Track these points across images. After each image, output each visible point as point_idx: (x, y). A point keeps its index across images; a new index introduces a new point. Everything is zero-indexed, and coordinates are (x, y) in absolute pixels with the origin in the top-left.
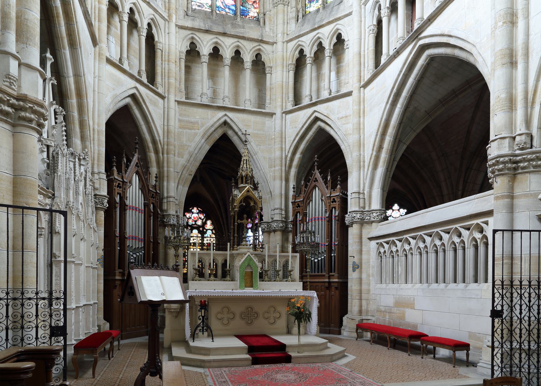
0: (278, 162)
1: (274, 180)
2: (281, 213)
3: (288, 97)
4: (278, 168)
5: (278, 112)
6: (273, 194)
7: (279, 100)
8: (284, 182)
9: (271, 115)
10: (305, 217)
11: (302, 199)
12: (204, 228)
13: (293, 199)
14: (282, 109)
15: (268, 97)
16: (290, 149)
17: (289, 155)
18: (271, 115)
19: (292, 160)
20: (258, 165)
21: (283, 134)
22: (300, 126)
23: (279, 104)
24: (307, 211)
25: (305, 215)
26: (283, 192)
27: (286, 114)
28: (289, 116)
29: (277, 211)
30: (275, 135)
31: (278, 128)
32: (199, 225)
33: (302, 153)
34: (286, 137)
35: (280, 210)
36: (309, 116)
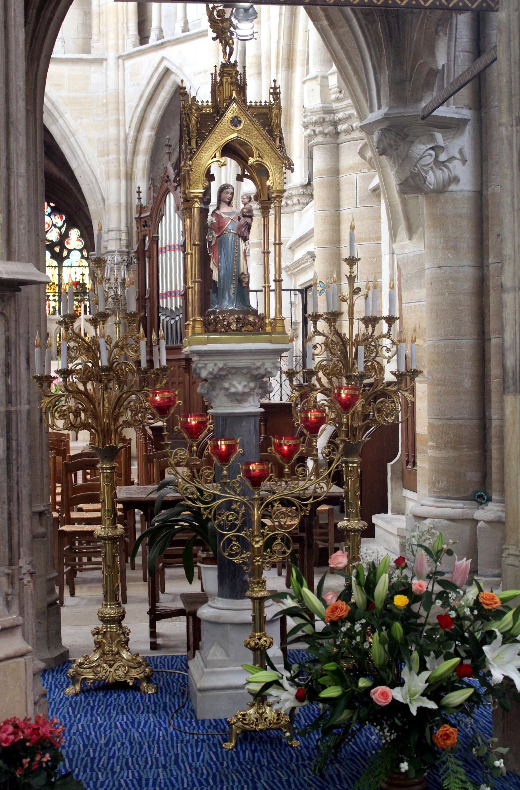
0: (112, 147)
1: (108, 178)
2: (119, 237)
3: (127, 27)
4: (113, 157)
5: (111, 56)
6: (106, 204)
7: (112, 36)
8: (123, 183)
9: (100, 61)
10: (155, 246)
11: (148, 214)
12: (63, 247)
13: (137, 213)
14: (117, 50)
15: (95, 30)
16: (131, 121)
17: (132, 133)
18: (100, 61)
19: (136, 140)
20: (80, 153)
21: (121, 97)
22: (145, 83)
23: (112, 42)
24: (158, 233)
25: (155, 240)
26: (123, 200)
27: (124, 59)
28: (129, 63)
29: (113, 235)
30: (106, 98)
31: (111, 86)
32: (52, 241)
33: (152, 128)
34: (126, 100)
35: (118, 233)
36: (156, 65)
